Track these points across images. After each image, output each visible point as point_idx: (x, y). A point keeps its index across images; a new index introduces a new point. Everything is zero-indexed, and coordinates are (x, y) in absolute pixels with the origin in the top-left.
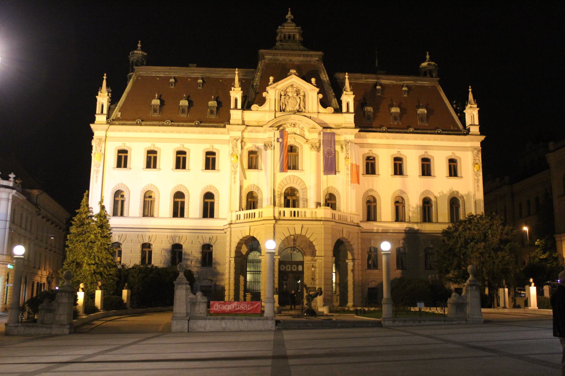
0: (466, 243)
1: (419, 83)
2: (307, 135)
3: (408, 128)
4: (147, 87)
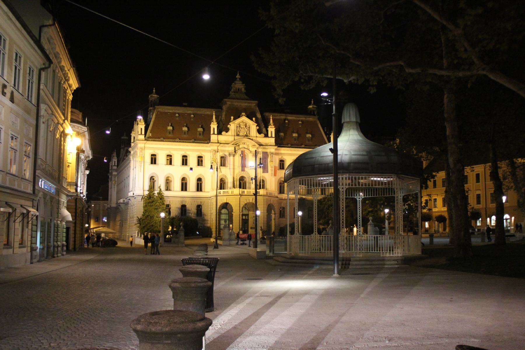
0: (329, 207)
1: (308, 119)
2: (251, 149)
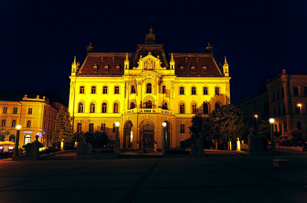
1: (204, 56)
3: (198, 75)
4: (93, 61)
